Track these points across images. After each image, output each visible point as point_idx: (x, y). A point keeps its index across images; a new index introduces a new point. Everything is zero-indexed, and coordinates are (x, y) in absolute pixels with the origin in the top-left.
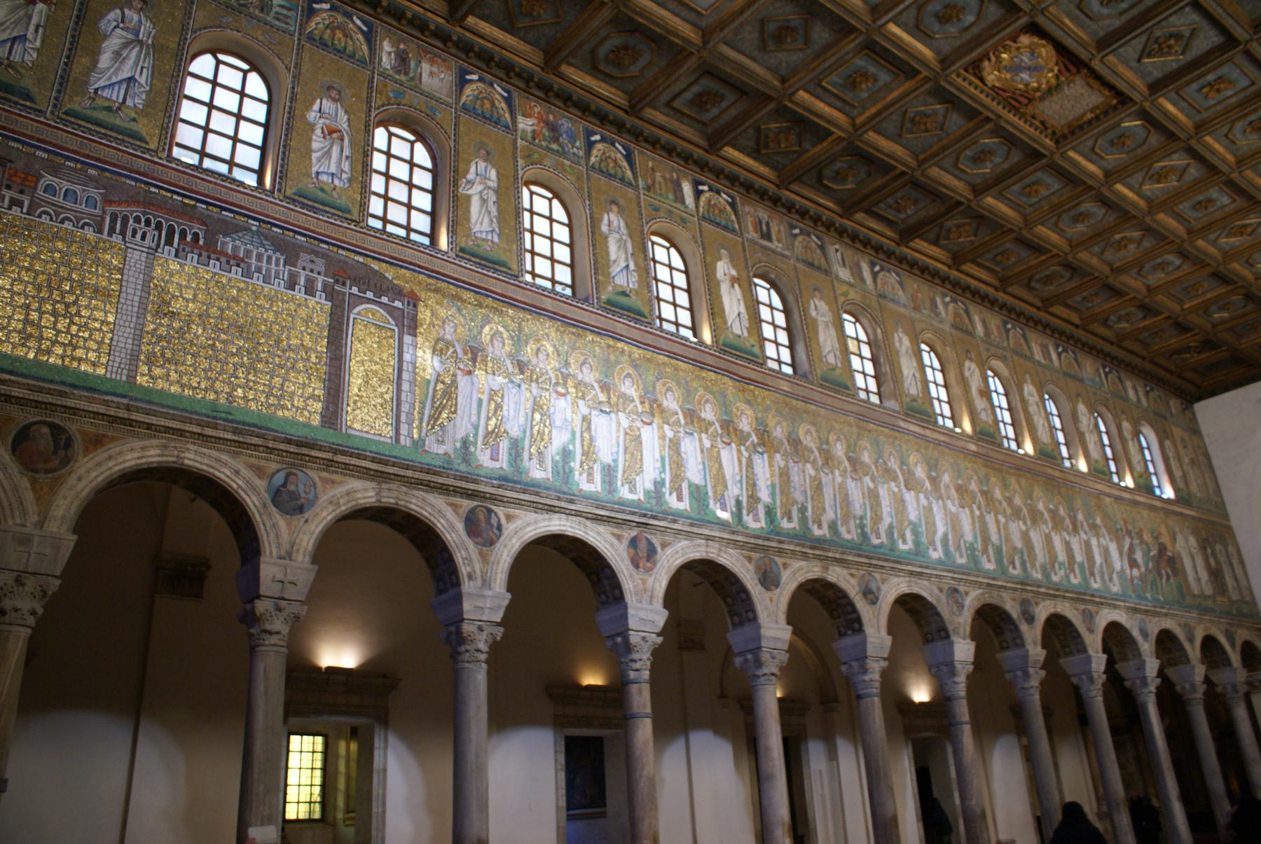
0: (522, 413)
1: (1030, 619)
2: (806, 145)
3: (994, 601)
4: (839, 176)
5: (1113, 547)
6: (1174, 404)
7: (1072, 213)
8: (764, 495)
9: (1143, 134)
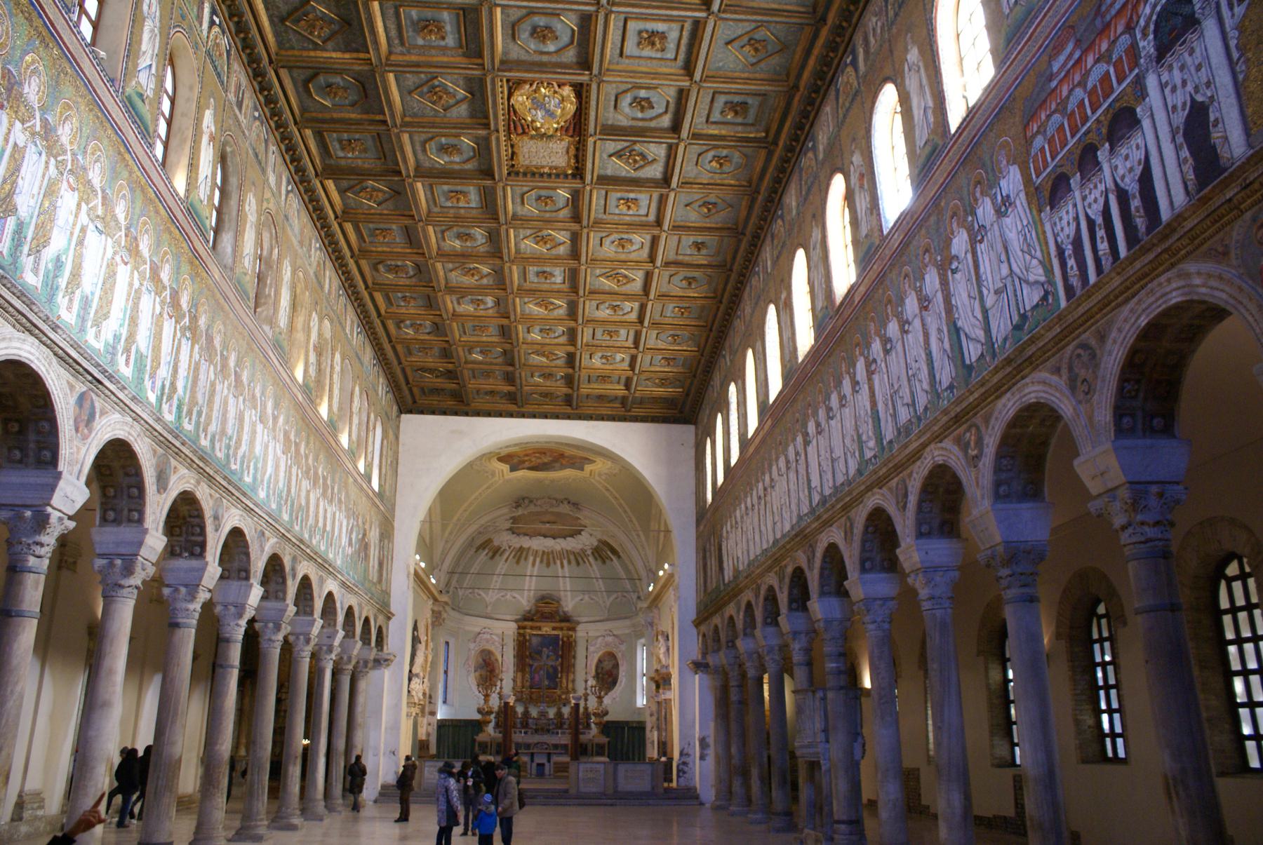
0: (35, 191)
1: (294, 576)
2: (330, 45)
3: (280, 553)
4: (328, 89)
5: (345, 523)
6: (395, 408)
7: (462, 230)
8: (180, 385)
9: (561, 203)
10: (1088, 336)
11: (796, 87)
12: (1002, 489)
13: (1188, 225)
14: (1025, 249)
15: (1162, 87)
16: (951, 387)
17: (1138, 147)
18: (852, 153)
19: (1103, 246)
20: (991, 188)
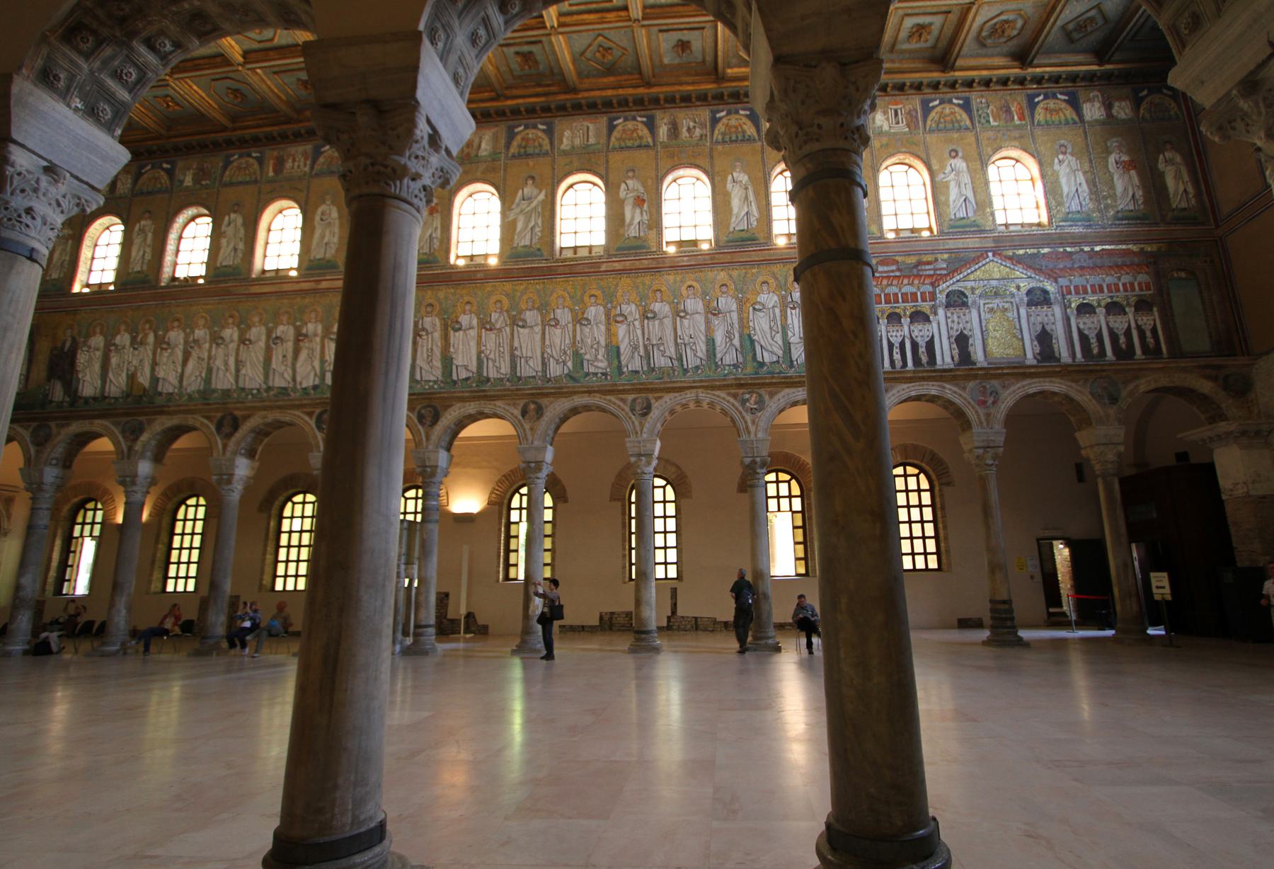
15: (947, 318)
19: (897, 357)
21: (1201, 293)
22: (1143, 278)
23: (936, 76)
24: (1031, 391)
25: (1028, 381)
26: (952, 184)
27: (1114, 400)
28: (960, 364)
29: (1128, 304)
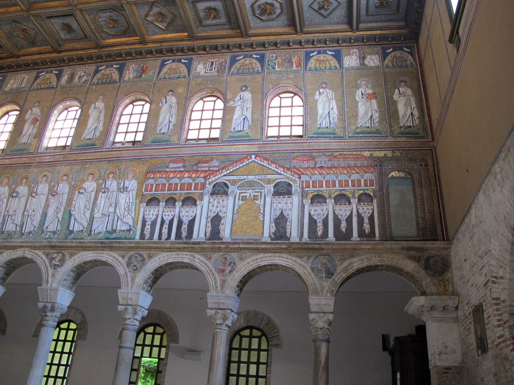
10: (145, 254)
11: (19, 57)
12: (65, 282)
13: (204, 246)
14: (127, 209)
16: (54, 233)
17: (193, 212)
18: (35, 106)
19: (165, 231)
20: (119, 179)
21: (414, 189)
22: (369, 176)
23: (238, 40)
24: (262, 264)
25: (262, 255)
26: (238, 108)
27: (330, 274)
28: (209, 239)
29: (354, 196)
